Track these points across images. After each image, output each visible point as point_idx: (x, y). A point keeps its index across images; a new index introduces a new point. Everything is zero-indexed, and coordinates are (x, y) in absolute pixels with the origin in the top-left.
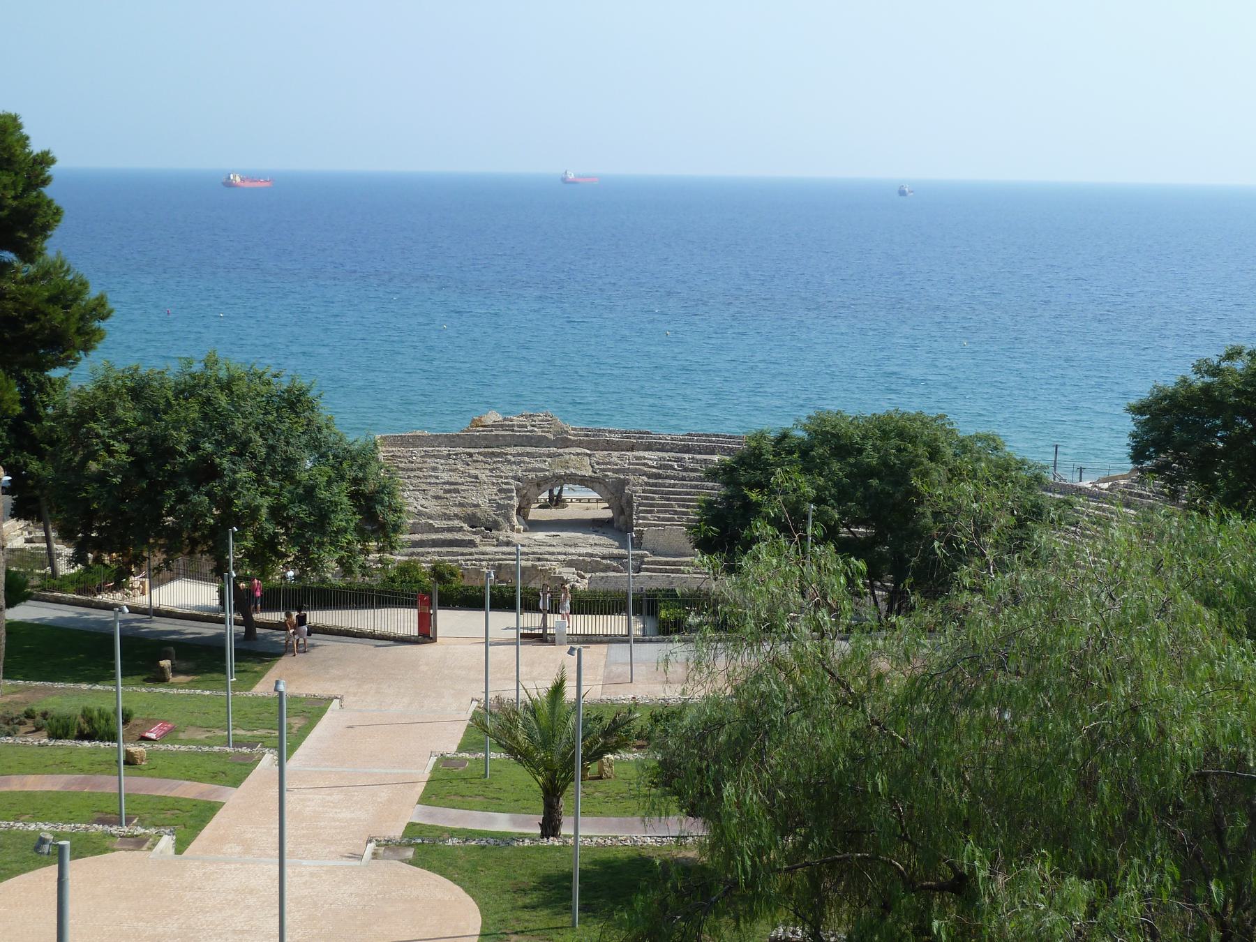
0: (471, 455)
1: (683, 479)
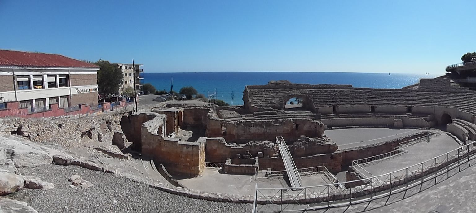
0: (270, 91)
1: (322, 95)
